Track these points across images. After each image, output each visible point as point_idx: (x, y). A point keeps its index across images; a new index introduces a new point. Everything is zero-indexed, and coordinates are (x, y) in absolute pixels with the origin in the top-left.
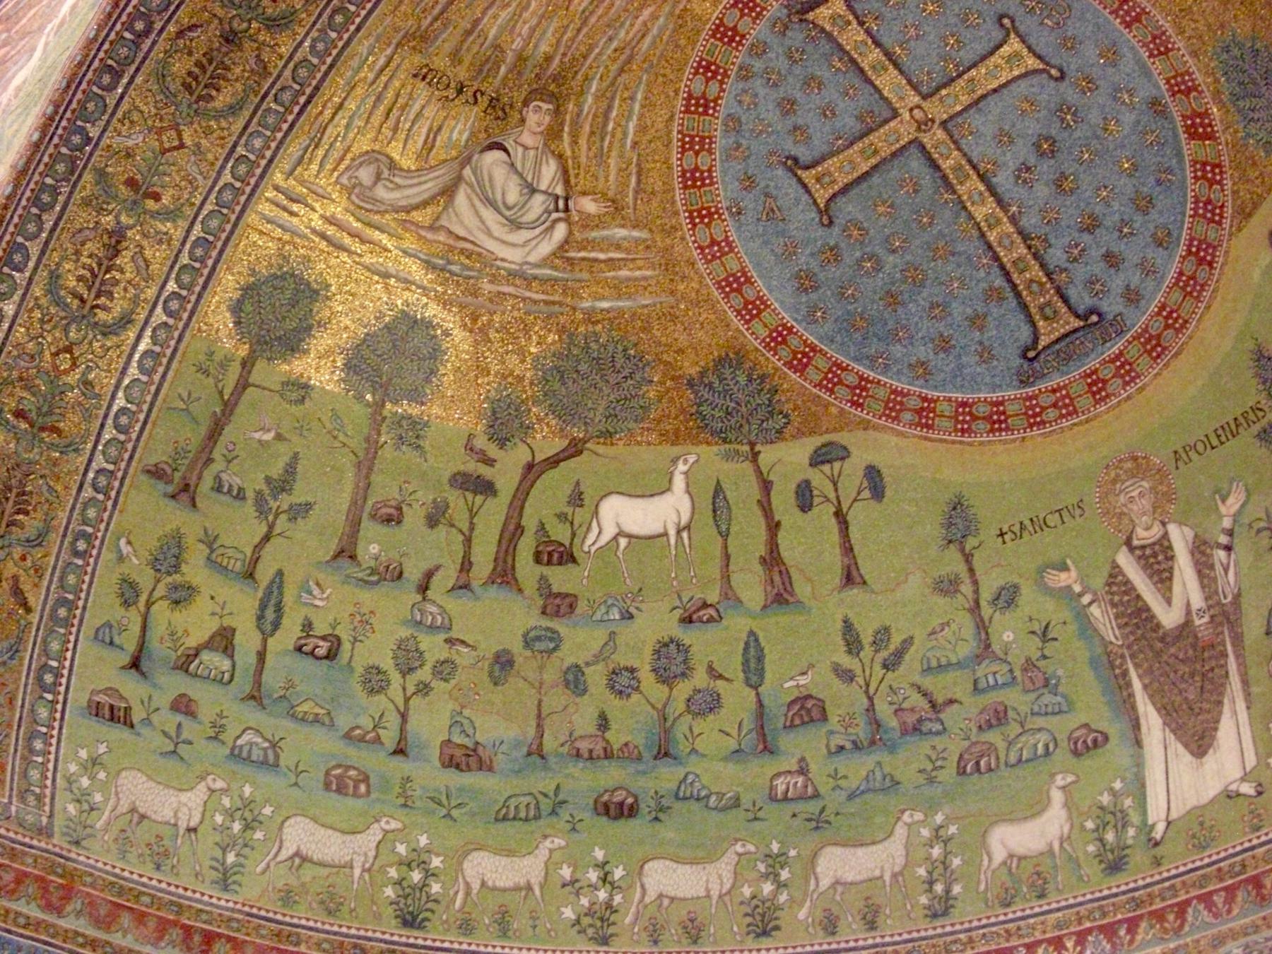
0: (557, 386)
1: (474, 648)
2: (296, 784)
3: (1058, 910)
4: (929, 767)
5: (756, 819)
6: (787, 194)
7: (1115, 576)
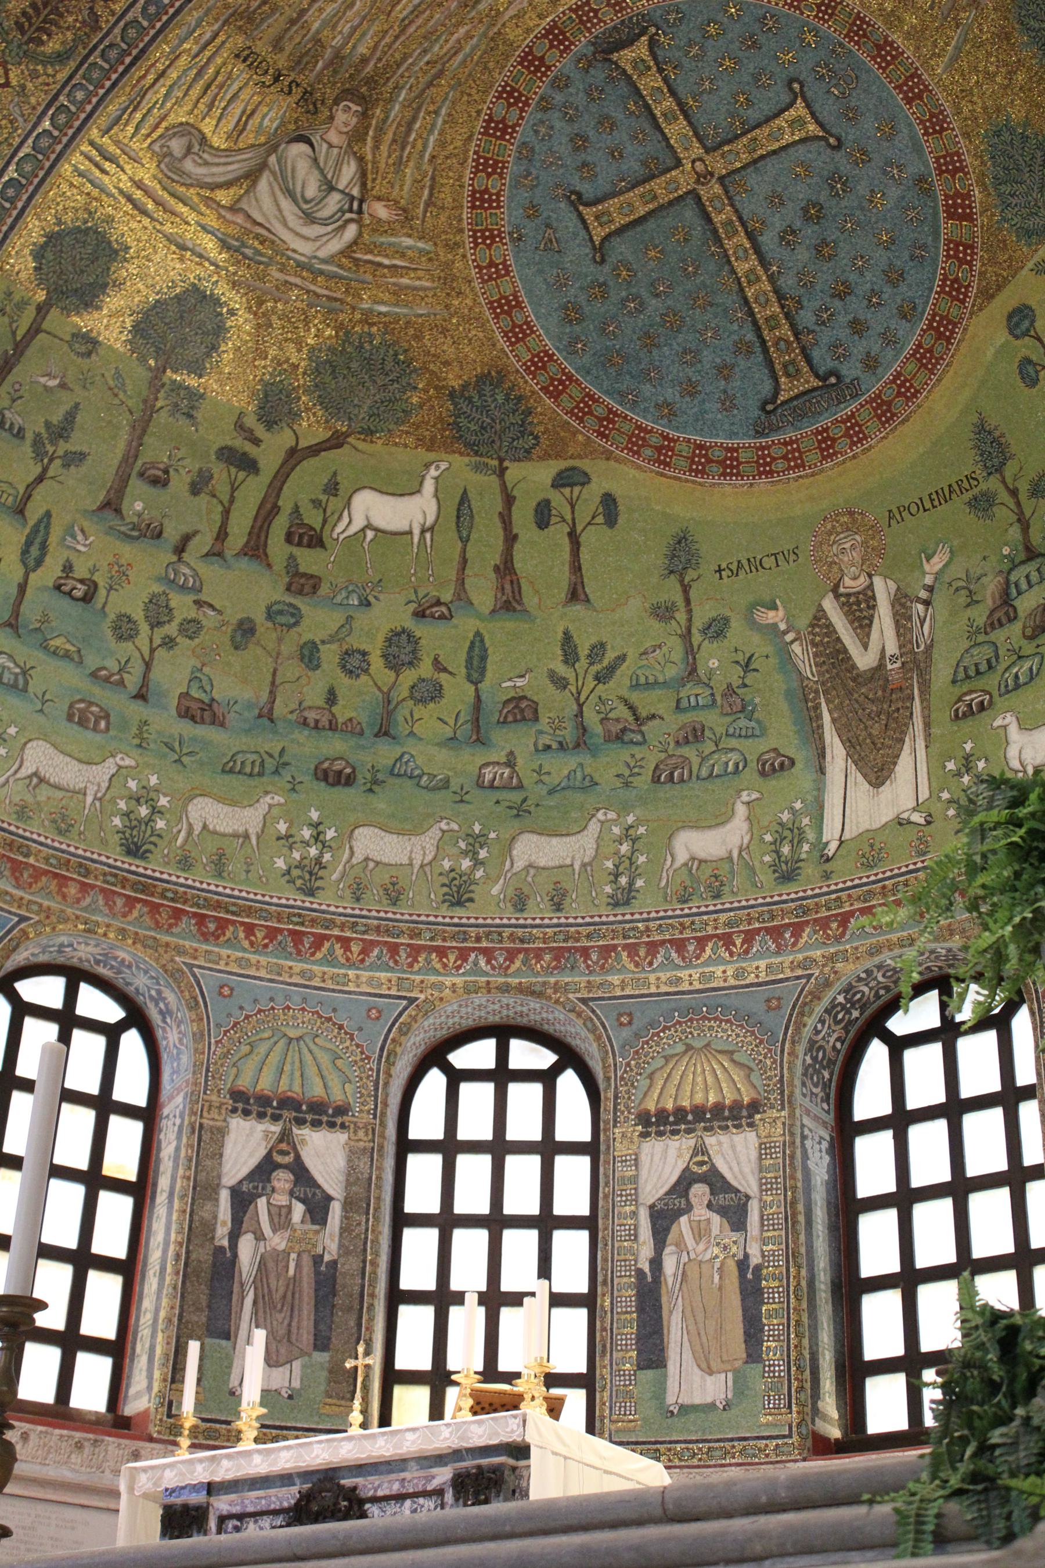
0: (328, 379)
1: (220, 612)
2: (41, 711)
3: (730, 910)
4: (627, 773)
5: (462, 801)
6: (567, 227)
7: (819, 620)
